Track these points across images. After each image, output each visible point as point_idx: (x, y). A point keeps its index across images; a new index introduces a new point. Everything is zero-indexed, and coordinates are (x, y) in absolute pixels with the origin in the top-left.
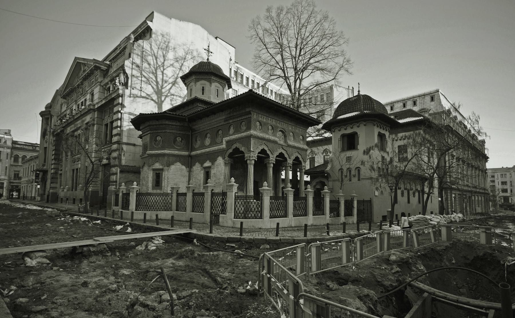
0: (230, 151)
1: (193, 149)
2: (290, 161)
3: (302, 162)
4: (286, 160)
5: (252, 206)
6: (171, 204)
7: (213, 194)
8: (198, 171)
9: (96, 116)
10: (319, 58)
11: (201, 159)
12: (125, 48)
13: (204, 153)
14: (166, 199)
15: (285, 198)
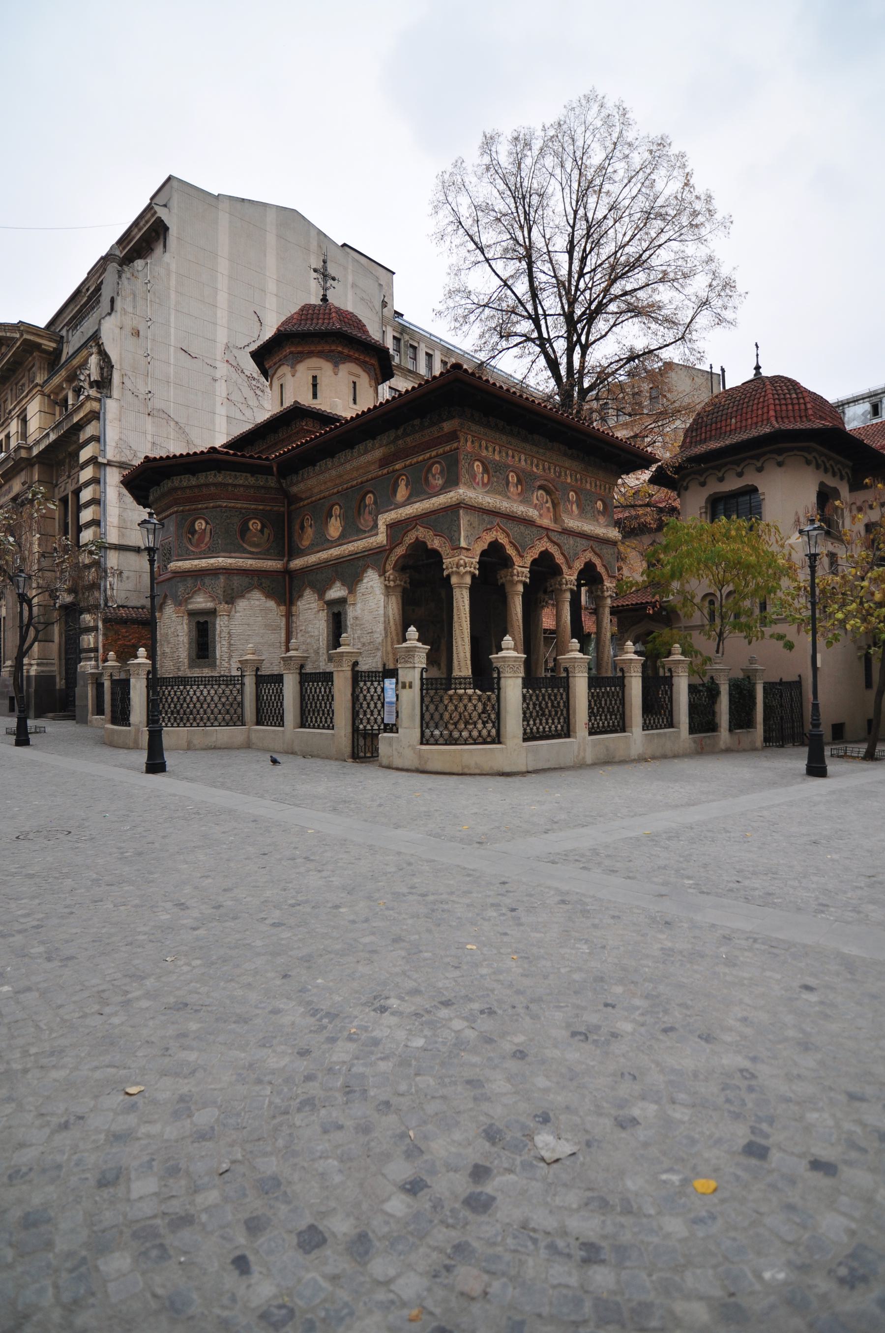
0: (400, 551)
1: (293, 552)
2: (570, 577)
3: (605, 577)
4: (556, 571)
5: (470, 707)
6: (241, 704)
7: (357, 677)
8: (312, 615)
9: (36, 478)
10: (639, 277)
11: (318, 579)
12: (98, 289)
13: (327, 561)
14: (228, 692)
15: (561, 682)
